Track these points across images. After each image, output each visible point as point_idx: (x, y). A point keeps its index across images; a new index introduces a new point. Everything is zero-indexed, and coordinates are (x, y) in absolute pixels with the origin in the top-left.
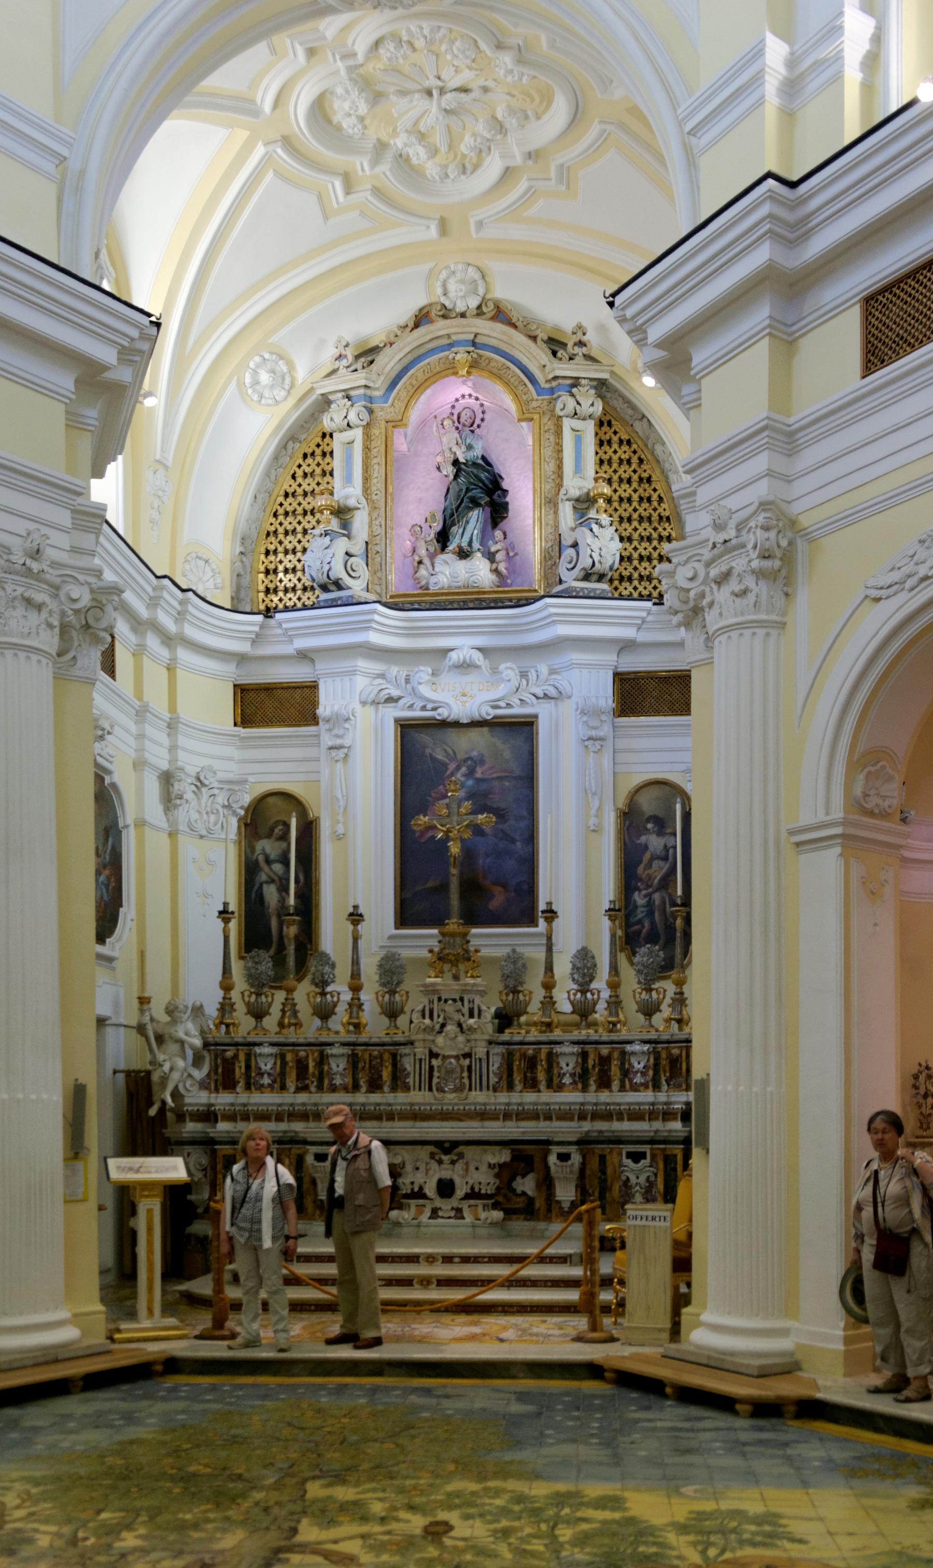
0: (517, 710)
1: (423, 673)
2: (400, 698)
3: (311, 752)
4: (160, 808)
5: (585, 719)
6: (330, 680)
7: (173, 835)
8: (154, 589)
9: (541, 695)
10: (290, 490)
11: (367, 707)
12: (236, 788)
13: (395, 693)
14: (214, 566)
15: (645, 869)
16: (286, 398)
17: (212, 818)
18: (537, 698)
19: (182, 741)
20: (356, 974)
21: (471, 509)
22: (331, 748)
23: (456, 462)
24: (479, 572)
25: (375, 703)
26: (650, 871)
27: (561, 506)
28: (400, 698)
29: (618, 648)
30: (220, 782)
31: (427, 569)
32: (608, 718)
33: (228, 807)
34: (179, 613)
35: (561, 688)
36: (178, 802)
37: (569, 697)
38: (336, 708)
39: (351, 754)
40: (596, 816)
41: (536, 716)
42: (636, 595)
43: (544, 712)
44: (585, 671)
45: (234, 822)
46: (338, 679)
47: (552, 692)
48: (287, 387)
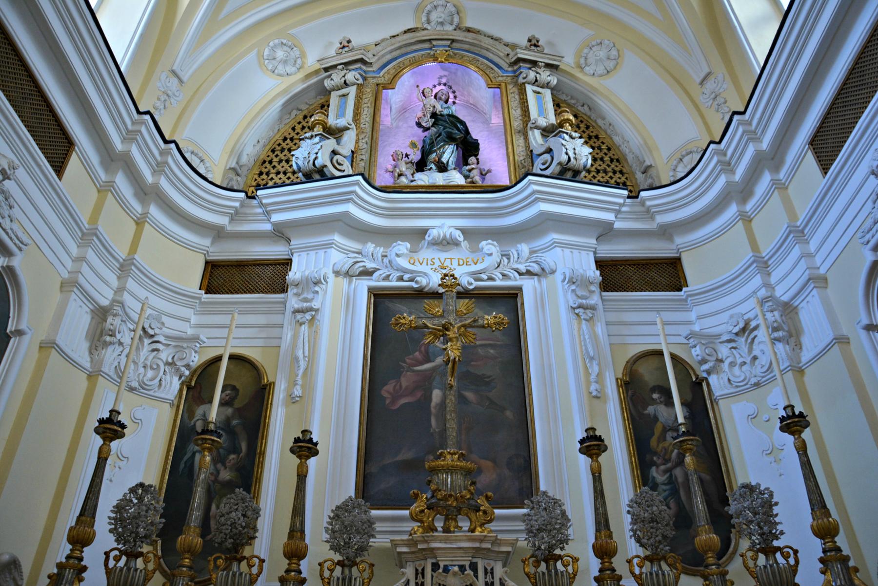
0: (499, 283)
1: (403, 247)
2: (377, 270)
3: (276, 319)
4: (85, 345)
5: (573, 287)
6: (304, 254)
7: (93, 376)
8: (133, 123)
9: (524, 271)
10: (289, 137)
11: (340, 279)
12: (185, 345)
13: (370, 265)
14: (208, 165)
15: (659, 442)
16: (295, 73)
17: (150, 374)
18: (520, 274)
19: (131, 284)
20: (297, 531)
21: (446, 143)
22: (297, 311)
23: (434, 115)
24: (456, 178)
25: (347, 274)
26: (666, 444)
27: (530, 133)
28: (377, 270)
29: (596, 235)
30: (167, 337)
31: (407, 178)
32: (595, 288)
33: (171, 364)
34: (158, 164)
35: (543, 266)
36: (108, 339)
37: (553, 272)
38: (307, 273)
39: (318, 317)
40: (597, 382)
41: (520, 289)
42: (613, 181)
43: (528, 286)
44: (567, 251)
45: (176, 384)
46: (312, 253)
47: (535, 268)
48: (298, 66)
